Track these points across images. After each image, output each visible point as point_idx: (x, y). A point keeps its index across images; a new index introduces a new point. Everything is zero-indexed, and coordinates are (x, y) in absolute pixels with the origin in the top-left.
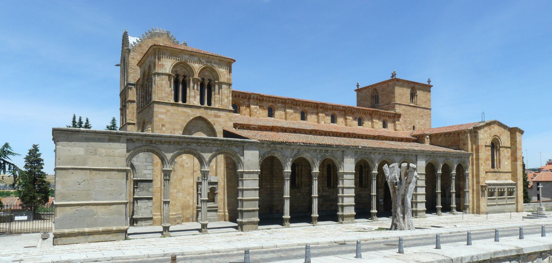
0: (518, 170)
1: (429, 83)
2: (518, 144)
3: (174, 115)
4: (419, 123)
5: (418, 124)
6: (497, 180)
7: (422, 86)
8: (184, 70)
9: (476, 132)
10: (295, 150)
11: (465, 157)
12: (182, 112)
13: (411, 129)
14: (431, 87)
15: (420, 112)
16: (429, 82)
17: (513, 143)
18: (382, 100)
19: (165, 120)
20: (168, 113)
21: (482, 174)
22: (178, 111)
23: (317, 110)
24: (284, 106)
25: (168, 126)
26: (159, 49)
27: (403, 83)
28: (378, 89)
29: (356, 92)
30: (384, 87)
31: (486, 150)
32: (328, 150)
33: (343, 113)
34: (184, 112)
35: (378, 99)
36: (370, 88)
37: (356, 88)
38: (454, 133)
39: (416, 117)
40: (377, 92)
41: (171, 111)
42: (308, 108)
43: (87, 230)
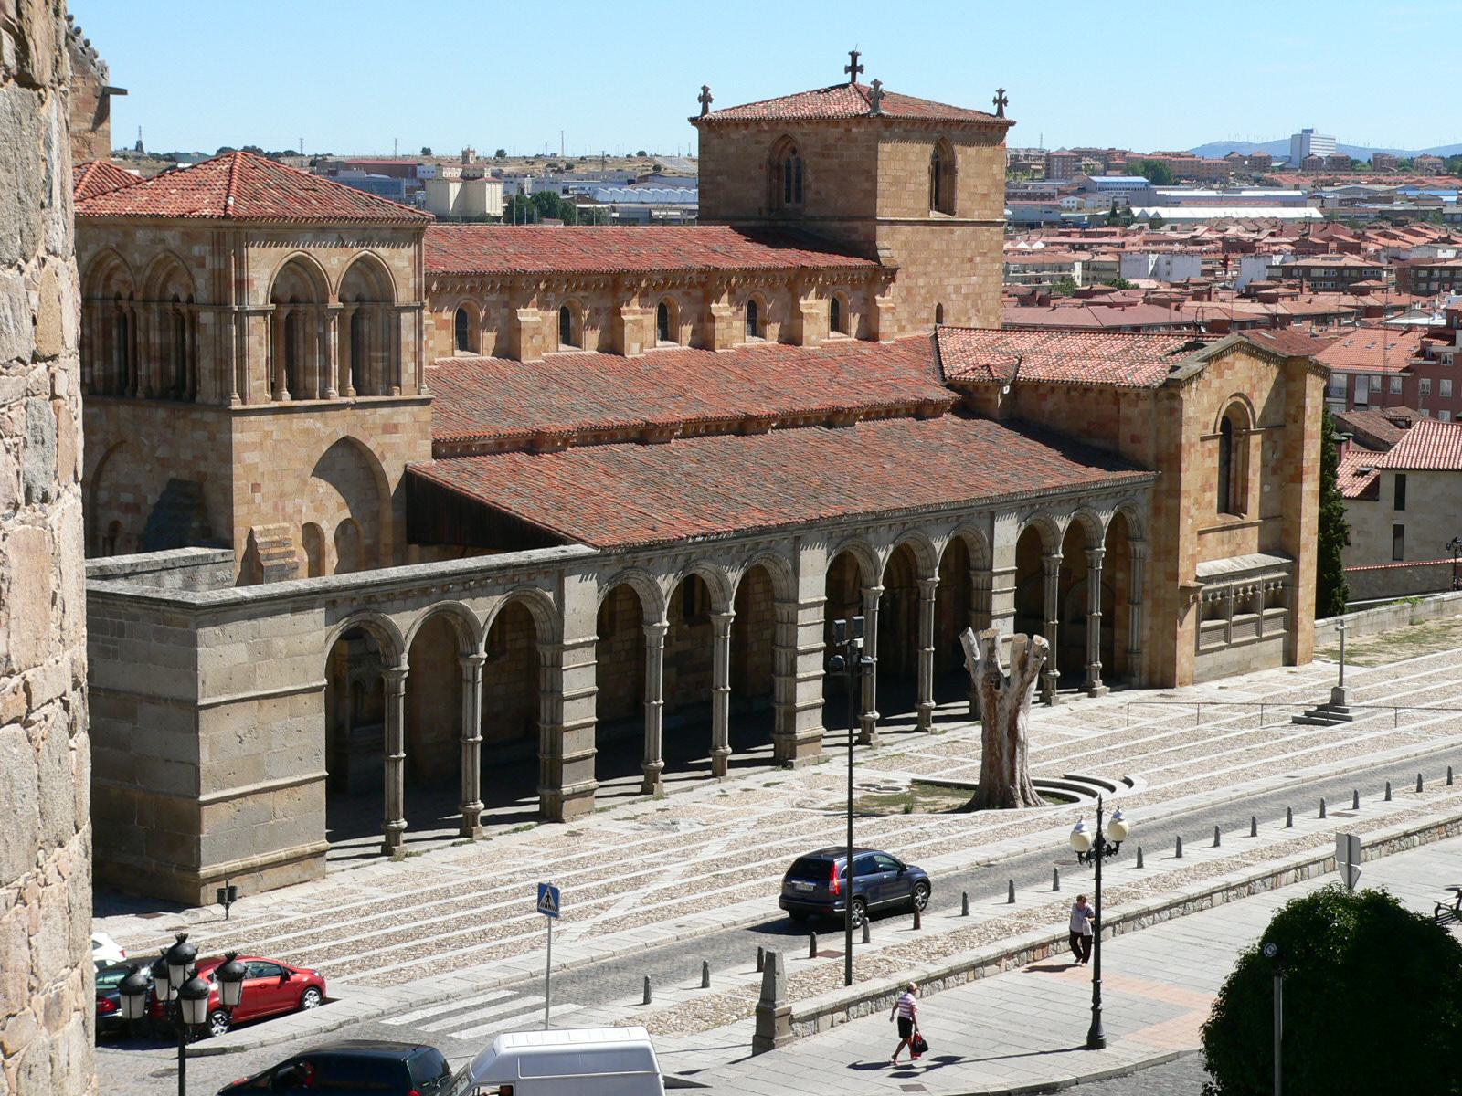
0: (1303, 513)
1: (1000, 112)
2: (1309, 418)
3: (282, 445)
4: (957, 289)
5: (953, 296)
6: (1233, 554)
7: (975, 130)
8: (293, 279)
9: (1175, 397)
10: (680, 557)
11: (1136, 490)
12: (301, 431)
13: (928, 321)
14: (1007, 129)
15: (965, 243)
16: (1001, 102)
17: (1293, 411)
18: (818, 193)
19: (260, 470)
20: (268, 443)
21: (1187, 544)
22: (291, 430)
23: (615, 296)
24: (506, 297)
25: (268, 487)
26: (237, 227)
27: (905, 131)
28: (800, 138)
29: (695, 131)
30: (831, 141)
31: (1203, 455)
32: (758, 544)
33: (698, 293)
34: (307, 432)
35: (798, 181)
36: (766, 128)
37: (696, 111)
38: (1101, 391)
39: (949, 265)
40: (794, 151)
41: (275, 437)
42: (582, 294)
43: (258, 859)
